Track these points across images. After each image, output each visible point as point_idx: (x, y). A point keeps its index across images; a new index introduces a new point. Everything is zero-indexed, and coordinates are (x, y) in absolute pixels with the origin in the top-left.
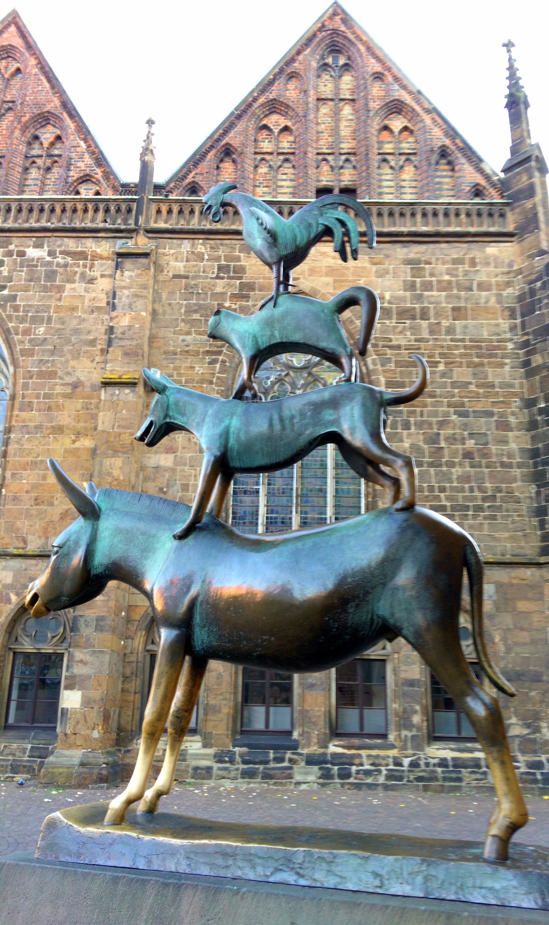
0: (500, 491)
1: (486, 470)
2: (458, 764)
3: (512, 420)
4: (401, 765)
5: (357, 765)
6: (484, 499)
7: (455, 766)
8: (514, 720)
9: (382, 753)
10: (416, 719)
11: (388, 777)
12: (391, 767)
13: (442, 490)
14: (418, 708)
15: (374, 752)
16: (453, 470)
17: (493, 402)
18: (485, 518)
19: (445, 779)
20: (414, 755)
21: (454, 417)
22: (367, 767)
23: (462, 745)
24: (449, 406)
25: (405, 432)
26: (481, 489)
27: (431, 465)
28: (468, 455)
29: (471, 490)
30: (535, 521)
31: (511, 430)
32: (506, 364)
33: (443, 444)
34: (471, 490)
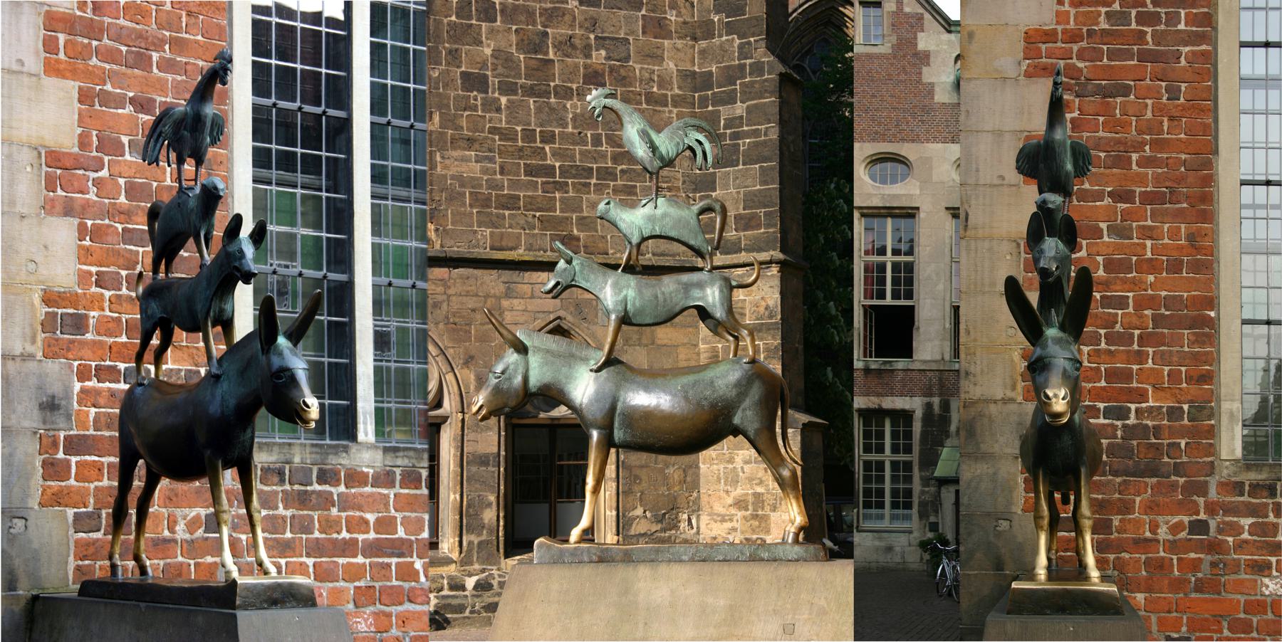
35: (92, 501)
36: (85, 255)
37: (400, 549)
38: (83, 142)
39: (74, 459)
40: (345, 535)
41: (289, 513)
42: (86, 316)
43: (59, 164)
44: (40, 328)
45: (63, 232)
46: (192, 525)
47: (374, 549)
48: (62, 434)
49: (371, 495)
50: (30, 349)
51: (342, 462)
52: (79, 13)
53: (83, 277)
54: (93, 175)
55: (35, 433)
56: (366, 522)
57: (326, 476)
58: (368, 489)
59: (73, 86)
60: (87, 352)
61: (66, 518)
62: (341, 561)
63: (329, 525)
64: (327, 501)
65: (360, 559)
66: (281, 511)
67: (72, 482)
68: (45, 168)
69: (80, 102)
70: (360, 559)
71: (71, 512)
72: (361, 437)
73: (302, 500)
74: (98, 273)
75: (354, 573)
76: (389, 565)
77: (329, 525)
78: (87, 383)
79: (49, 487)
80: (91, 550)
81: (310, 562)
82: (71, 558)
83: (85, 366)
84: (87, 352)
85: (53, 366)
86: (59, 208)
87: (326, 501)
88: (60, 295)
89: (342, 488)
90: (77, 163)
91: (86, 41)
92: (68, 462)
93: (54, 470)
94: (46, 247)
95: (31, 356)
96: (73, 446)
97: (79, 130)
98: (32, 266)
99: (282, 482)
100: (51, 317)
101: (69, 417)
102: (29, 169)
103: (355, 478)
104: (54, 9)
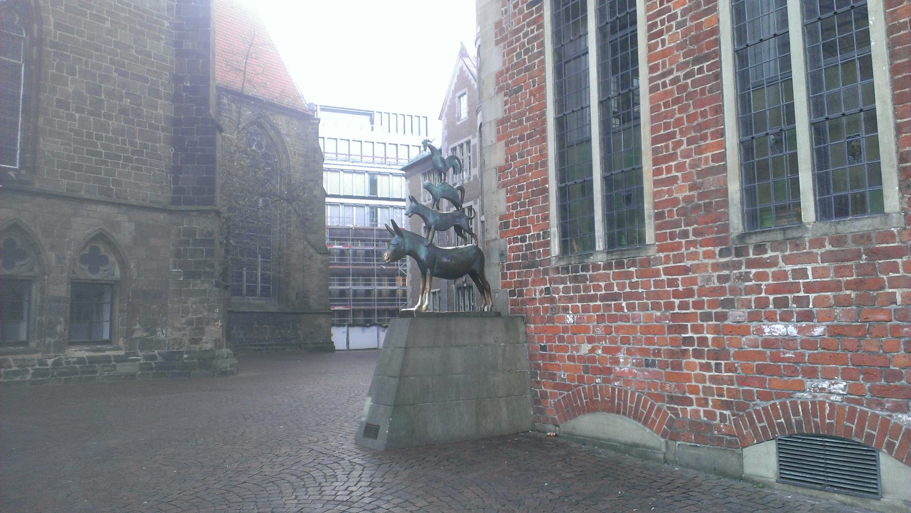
0: (147, 148)
1: (138, 128)
2: (92, 360)
3: (162, 89)
4: (46, 365)
5: (5, 368)
6: (133, 152)
7: (90, 362)
8: (138, 326)
9: (27, 357)
10: (60, 328)
11: (34, 375)
12: (37, 367)
13: (99, 138)
14: (62, 319)
15: (20, 357)
16: (110, 122)
17: (148, 70)
18: (132, 168)
19: (83, 373)
20: (56, 356)
21: (115, 75)
22: (14, 368)
23: (94, 347)
24: (111, 63)
25: (70, 77)
26: (132, 143)
27: (91, 113)
28: (123, 111)
29: (124, 142)
30: (170, 177)
31: (161, 99)
32: (161, 39)
33: (103, 97)
34: (124, 142)
37: (615, 297)
38: (507, 160)
40: (592, 292)
41: (571, 285)
45: (502, 194)
46: (541, 292)
47: (604, 298)
49: (601, 274)
51: (592, 259)
53: (508, 208)
56: (601, 286)
57: (585, 268)
58: (602, 271)
59: (503, 142)
62: (591, 304)
63: (587, 289)
64: (584, 279)
65: (599, 303)
66: (568, 284)
70: (599, 303)
72: (597, 249)
73: (575, 279)
75: (597, 309)
76: (610, 305)
77: (587, 289)
81: (580, 305)
85: (502, 241)
87: (584, 279)
89: (591, 273)
93: (504, 276)
96: (509, 267)
99: (568, 272)
103: (596, 267)
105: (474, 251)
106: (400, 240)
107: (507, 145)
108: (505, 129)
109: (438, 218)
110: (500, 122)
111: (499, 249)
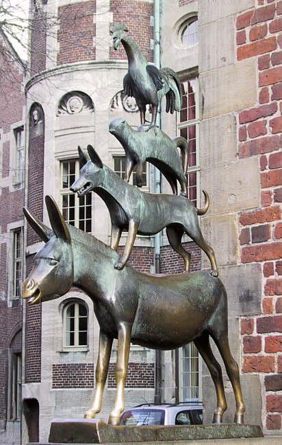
35: (276, 367)
36: (266, 180)
38: (263, 98)
39: (264, 336)
42: (268, 226)
43: (247, 120)
44: (238, 241)
45: (251, 169)
48: (255, 319)
50: (232, 258)
52: (260, 6)
53: (266, 197)
54: (269, 119)
55: (238, 319)
59: (254, 60)
60: (269, 254)
61: (259, 380)
67: (263, 353)
68: (239, 126)
69: (260, 69)
71: (262, 376)
74: (276, 191)
78: (272, 277)
79: (248, 358)
80: (277, 404)
82: (264, 410)
83: (268, 264)
84: (269, 254)
85: (248, 268)
86: (247, 152)
88: (250, 216)
90: (261, 113)
91: (263, 24)
92: (259, 338)
93: (252, 345)
94: (240, 182)
95: (234, 263)
96: (265, 326)
97: (259, 90)
98: (231, 200)
100: (245, 232)
101: (258, 304)
102: (229, 131)
104: (243, 13)
105: (211, 287)
106: (64, 247)
107: (263, 64)
108: (256, 35)
109: (141, 203)
110: (243, 21)
111: (239, 286)
